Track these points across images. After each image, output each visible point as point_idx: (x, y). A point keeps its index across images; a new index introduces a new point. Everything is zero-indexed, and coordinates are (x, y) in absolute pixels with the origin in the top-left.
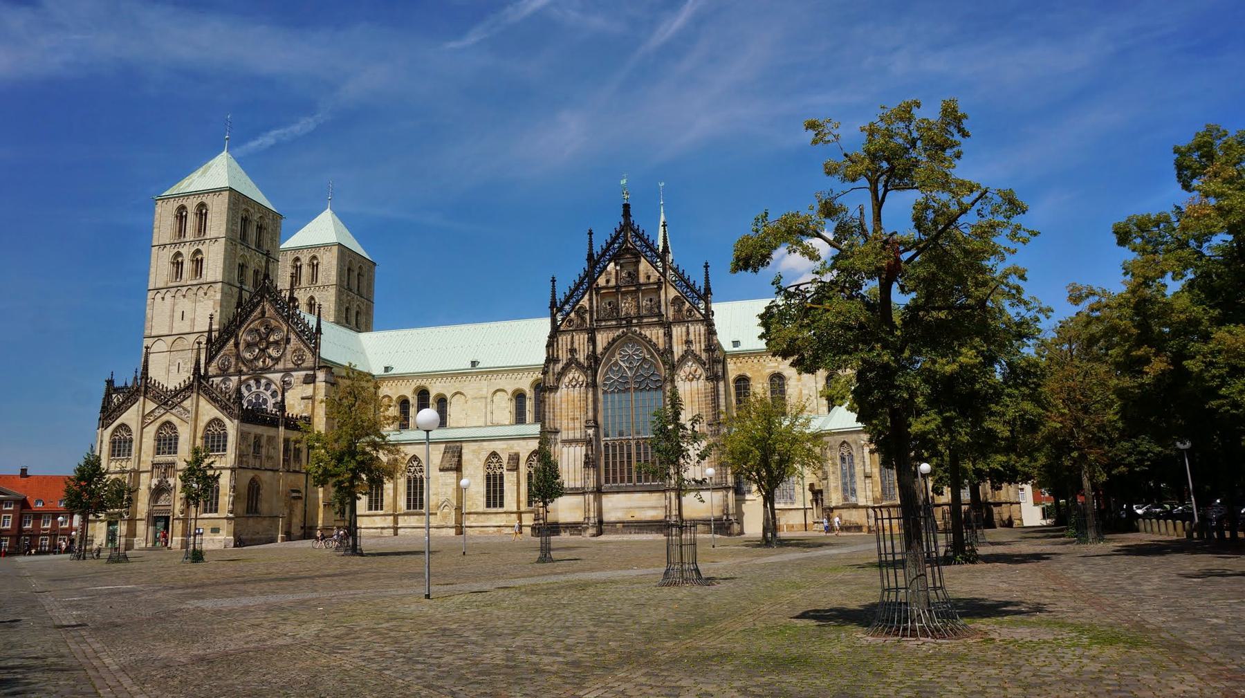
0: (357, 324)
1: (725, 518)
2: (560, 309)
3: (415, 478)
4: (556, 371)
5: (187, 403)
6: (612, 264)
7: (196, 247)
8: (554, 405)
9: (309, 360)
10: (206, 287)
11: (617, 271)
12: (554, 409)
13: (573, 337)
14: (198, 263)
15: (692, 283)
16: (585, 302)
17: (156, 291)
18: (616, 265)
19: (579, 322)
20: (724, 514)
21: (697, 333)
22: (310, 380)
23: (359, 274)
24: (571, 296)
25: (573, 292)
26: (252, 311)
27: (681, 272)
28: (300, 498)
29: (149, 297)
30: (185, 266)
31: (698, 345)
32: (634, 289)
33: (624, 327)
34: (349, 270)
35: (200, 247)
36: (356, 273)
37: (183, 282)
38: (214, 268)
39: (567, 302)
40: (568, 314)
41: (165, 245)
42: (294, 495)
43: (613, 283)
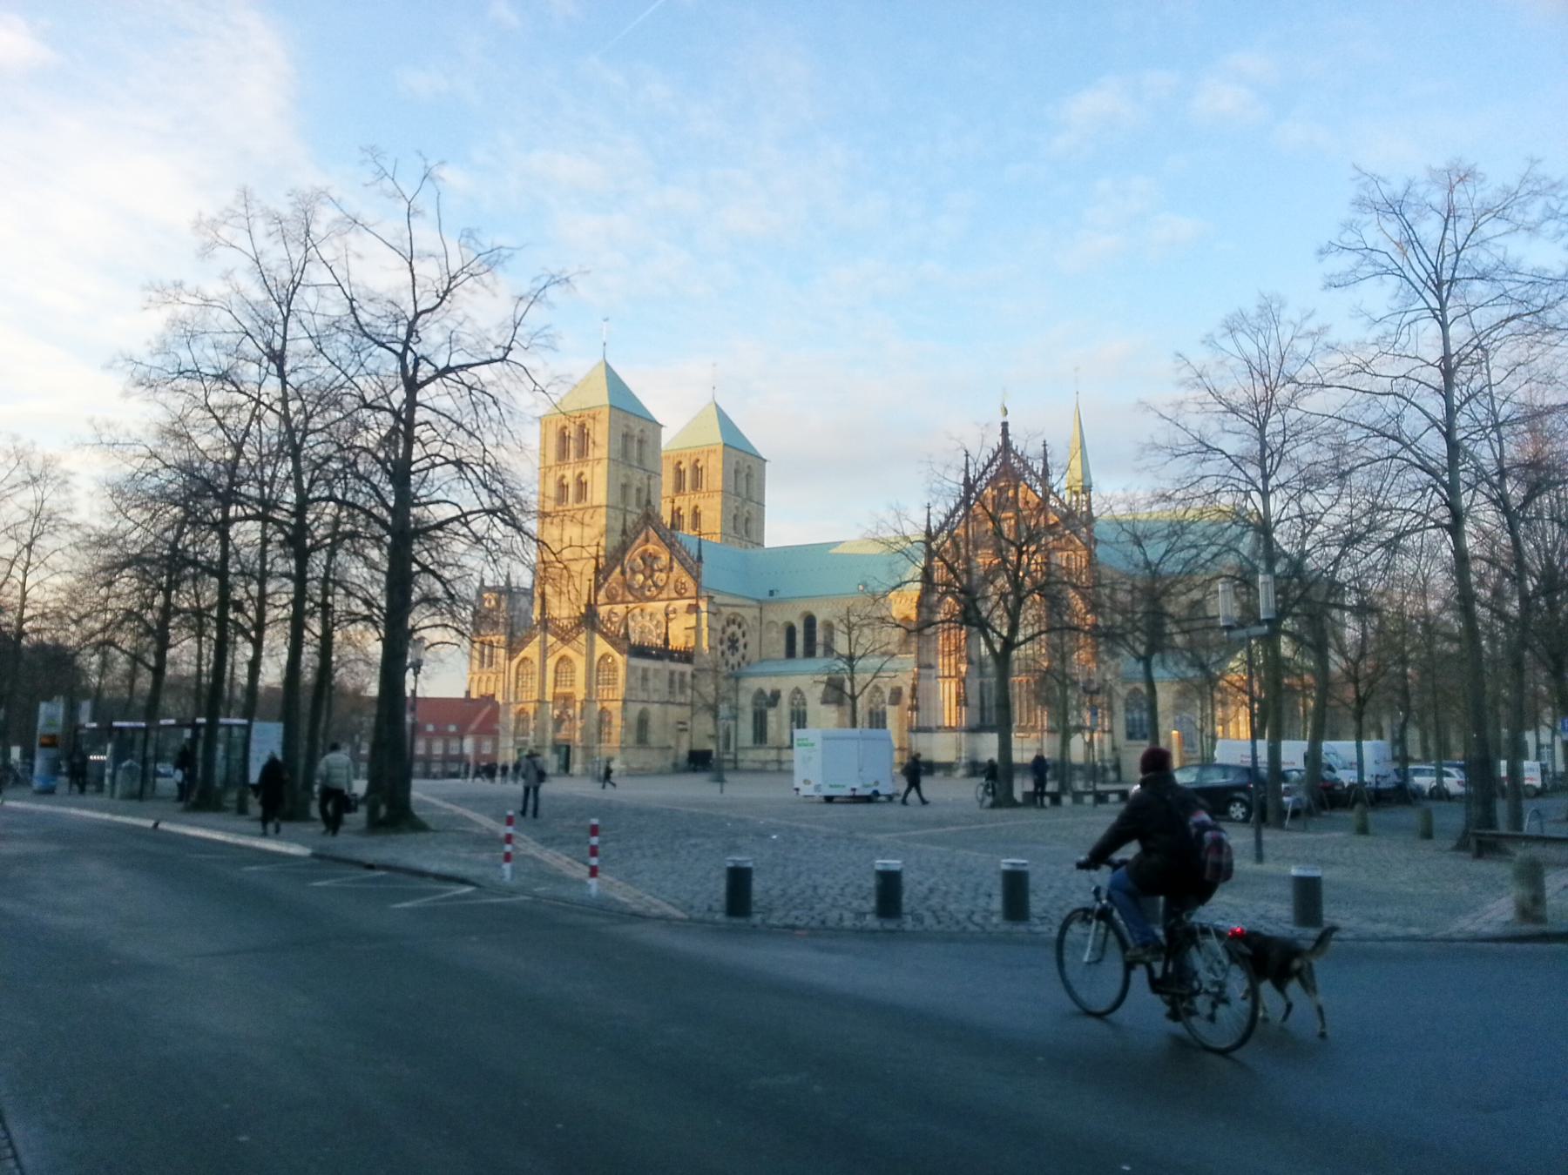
0: (747, 532)
3: (799, 712)
5: (582, 638)
6: (989, 489)
10: (591, 511)
14: (582, 485)
22: (694, 609)
23: (747, 475)
26: (636, 538)
34: (736, 472)
36: (744, 475)
37: (569, 507)
38: (599, 493)
39: (941, 529)
40: (943, 543)
41: (550, 468)
42: (681, 726)
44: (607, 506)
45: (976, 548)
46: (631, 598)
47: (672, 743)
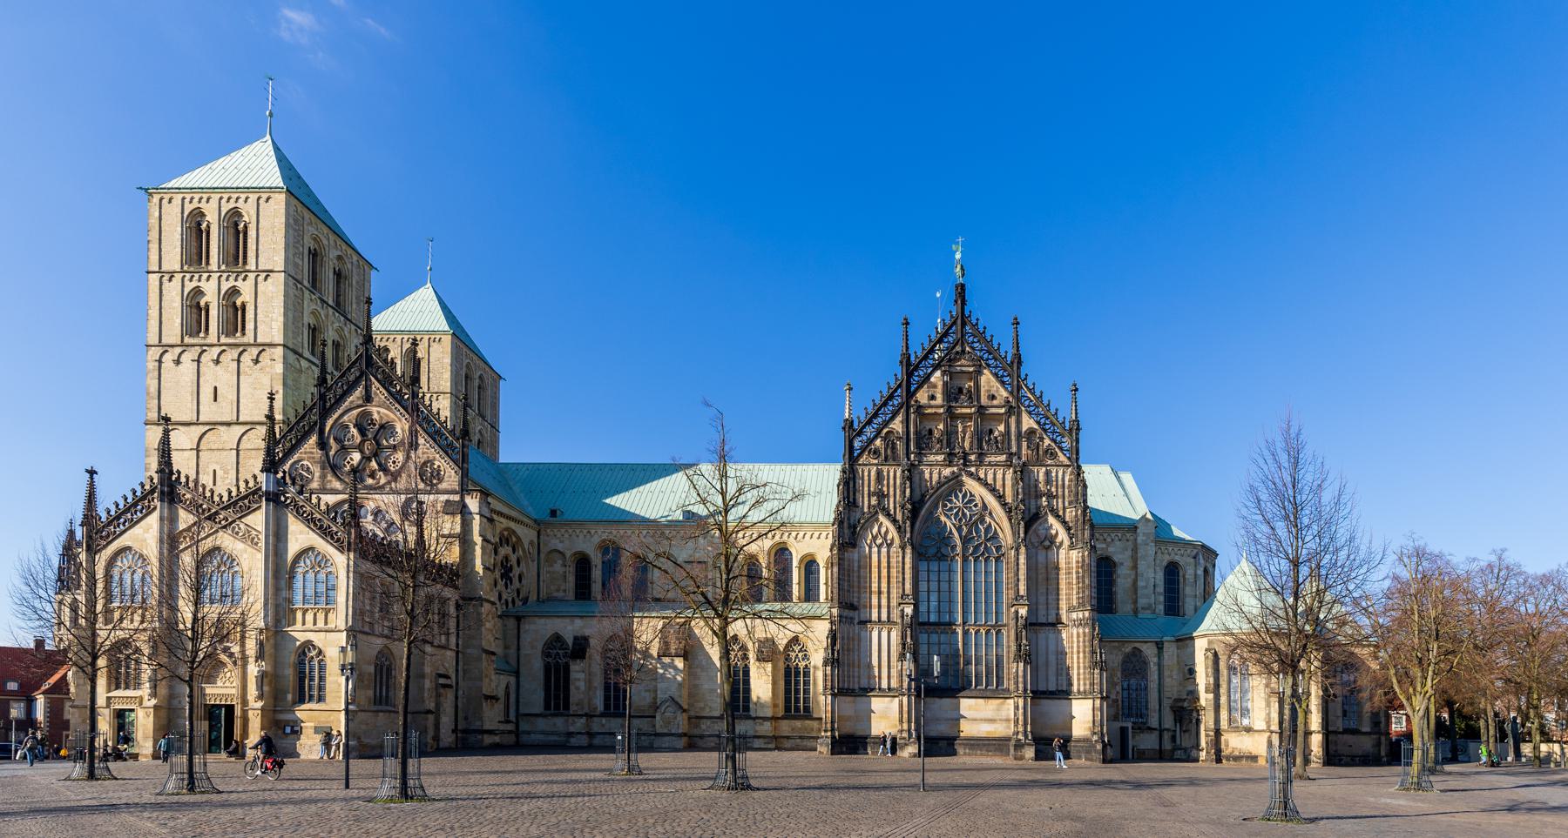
1: (1095, 738)
2: (860, 433)
4: (852, 521)
7: (232, 283)
8: (849, 570)
9: (451, 478)
10: (255, 351)
11: (945, 384)
12: (849, 575)
13: (879, 473)
15: (1053, 411)
16: (897, 425)
17: (161, 350)
18: (944, 373)
19: (889, 452)
20: (1095, 733)
21: (1060, 483)
24: (876, 415)
25: (879, 409)
26: (346, 394)
27: (1038, 394)
28: (450, 686)
29: (149, 358)
30: (213, 313)
31: (1060, 501)
32: (968, 411)
33: (954, 466)
35: (239, 284)
39: (869, 422)
40: (871, 441)
43: (939, 400)
44: (284, 346)
45: (920, 454)
46: (337, 485)
47: (432, 706)
